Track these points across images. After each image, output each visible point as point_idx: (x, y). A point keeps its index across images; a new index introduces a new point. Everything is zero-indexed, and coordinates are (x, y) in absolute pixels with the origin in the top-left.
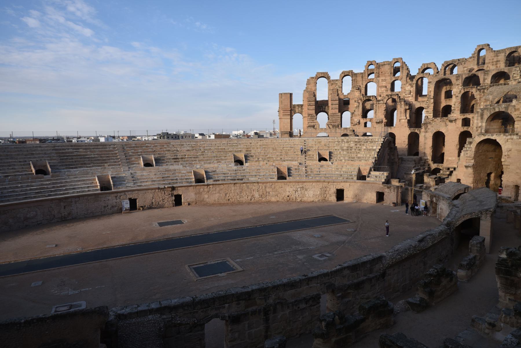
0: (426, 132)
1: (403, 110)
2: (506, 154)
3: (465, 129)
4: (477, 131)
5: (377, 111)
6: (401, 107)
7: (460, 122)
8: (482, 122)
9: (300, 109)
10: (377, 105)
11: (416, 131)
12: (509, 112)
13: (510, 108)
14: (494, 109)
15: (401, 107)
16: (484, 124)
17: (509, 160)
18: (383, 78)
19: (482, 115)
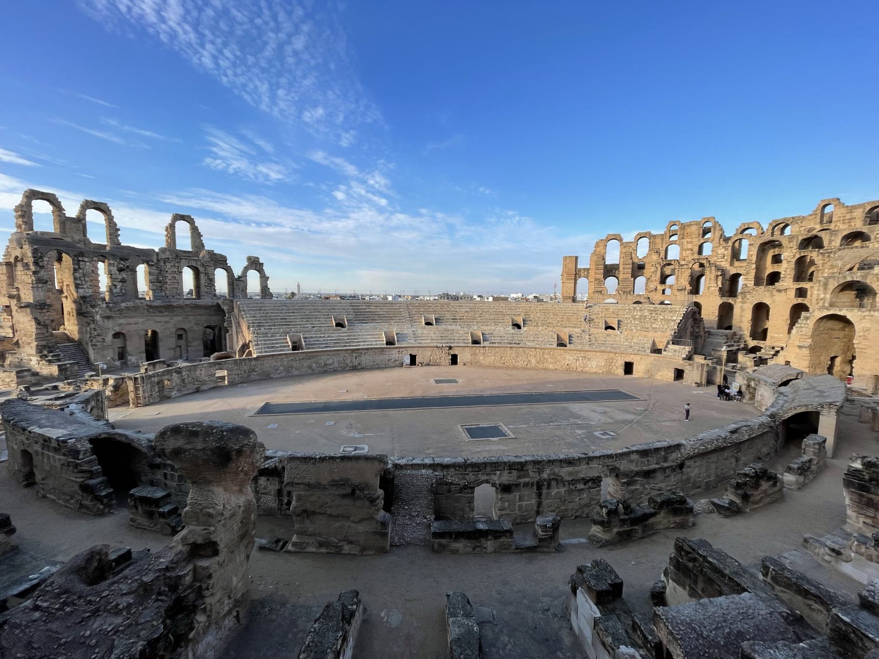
0: (744, 303)
1: (713, 276)
2: (862, 334)
7: (792, 293)
8: (825, 294)
13: (870, 277)
14: (845, 277)
16: (828, 296)
17: (865, 342)
19: (826, 285)
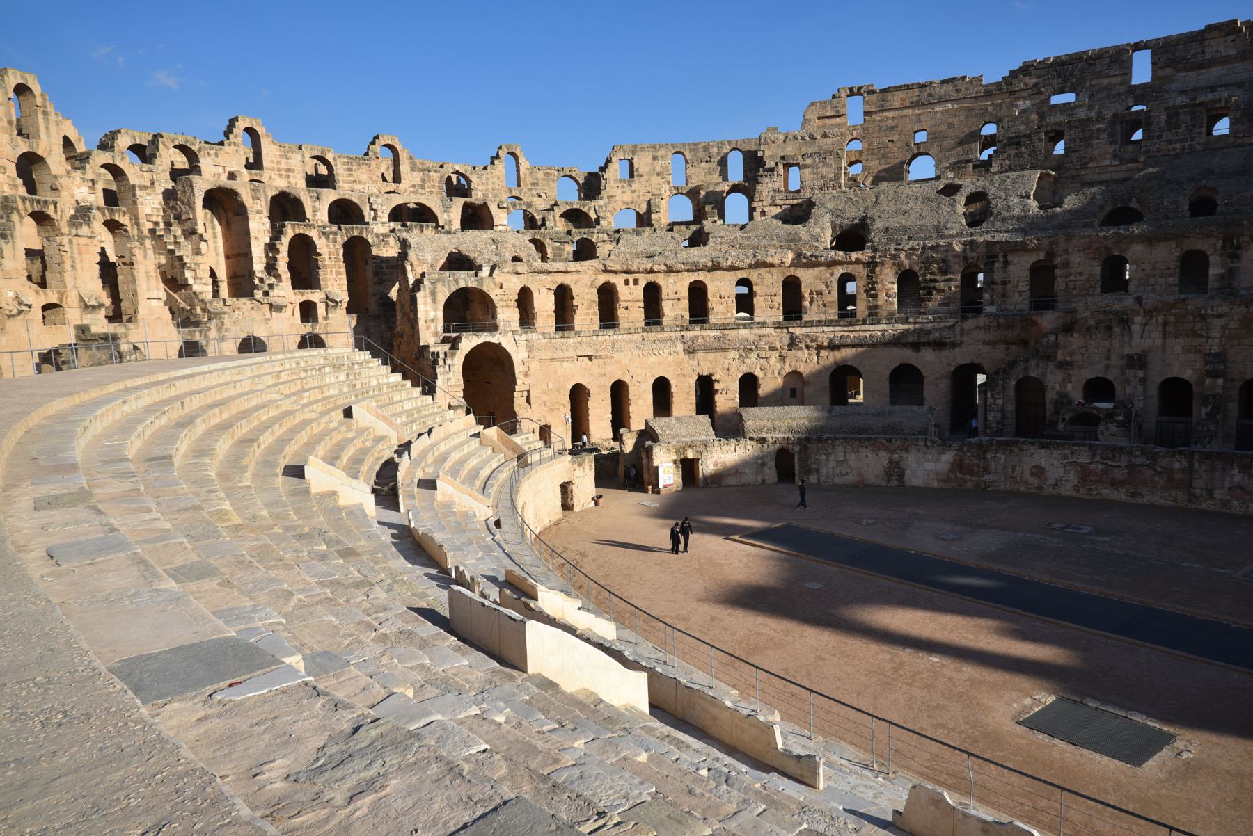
0: (223, 339)
3: (306, 329)
4: (428, 328)
5: (78, 266)
6: (145, 257)
8: (435, 310)
10: (75, 240)
11: (197, 337)
12: (485, 289)
13: (486, 282)
14: (457, 281)
15: (145, 257)
17: (528, 381)
19: (433, 294)
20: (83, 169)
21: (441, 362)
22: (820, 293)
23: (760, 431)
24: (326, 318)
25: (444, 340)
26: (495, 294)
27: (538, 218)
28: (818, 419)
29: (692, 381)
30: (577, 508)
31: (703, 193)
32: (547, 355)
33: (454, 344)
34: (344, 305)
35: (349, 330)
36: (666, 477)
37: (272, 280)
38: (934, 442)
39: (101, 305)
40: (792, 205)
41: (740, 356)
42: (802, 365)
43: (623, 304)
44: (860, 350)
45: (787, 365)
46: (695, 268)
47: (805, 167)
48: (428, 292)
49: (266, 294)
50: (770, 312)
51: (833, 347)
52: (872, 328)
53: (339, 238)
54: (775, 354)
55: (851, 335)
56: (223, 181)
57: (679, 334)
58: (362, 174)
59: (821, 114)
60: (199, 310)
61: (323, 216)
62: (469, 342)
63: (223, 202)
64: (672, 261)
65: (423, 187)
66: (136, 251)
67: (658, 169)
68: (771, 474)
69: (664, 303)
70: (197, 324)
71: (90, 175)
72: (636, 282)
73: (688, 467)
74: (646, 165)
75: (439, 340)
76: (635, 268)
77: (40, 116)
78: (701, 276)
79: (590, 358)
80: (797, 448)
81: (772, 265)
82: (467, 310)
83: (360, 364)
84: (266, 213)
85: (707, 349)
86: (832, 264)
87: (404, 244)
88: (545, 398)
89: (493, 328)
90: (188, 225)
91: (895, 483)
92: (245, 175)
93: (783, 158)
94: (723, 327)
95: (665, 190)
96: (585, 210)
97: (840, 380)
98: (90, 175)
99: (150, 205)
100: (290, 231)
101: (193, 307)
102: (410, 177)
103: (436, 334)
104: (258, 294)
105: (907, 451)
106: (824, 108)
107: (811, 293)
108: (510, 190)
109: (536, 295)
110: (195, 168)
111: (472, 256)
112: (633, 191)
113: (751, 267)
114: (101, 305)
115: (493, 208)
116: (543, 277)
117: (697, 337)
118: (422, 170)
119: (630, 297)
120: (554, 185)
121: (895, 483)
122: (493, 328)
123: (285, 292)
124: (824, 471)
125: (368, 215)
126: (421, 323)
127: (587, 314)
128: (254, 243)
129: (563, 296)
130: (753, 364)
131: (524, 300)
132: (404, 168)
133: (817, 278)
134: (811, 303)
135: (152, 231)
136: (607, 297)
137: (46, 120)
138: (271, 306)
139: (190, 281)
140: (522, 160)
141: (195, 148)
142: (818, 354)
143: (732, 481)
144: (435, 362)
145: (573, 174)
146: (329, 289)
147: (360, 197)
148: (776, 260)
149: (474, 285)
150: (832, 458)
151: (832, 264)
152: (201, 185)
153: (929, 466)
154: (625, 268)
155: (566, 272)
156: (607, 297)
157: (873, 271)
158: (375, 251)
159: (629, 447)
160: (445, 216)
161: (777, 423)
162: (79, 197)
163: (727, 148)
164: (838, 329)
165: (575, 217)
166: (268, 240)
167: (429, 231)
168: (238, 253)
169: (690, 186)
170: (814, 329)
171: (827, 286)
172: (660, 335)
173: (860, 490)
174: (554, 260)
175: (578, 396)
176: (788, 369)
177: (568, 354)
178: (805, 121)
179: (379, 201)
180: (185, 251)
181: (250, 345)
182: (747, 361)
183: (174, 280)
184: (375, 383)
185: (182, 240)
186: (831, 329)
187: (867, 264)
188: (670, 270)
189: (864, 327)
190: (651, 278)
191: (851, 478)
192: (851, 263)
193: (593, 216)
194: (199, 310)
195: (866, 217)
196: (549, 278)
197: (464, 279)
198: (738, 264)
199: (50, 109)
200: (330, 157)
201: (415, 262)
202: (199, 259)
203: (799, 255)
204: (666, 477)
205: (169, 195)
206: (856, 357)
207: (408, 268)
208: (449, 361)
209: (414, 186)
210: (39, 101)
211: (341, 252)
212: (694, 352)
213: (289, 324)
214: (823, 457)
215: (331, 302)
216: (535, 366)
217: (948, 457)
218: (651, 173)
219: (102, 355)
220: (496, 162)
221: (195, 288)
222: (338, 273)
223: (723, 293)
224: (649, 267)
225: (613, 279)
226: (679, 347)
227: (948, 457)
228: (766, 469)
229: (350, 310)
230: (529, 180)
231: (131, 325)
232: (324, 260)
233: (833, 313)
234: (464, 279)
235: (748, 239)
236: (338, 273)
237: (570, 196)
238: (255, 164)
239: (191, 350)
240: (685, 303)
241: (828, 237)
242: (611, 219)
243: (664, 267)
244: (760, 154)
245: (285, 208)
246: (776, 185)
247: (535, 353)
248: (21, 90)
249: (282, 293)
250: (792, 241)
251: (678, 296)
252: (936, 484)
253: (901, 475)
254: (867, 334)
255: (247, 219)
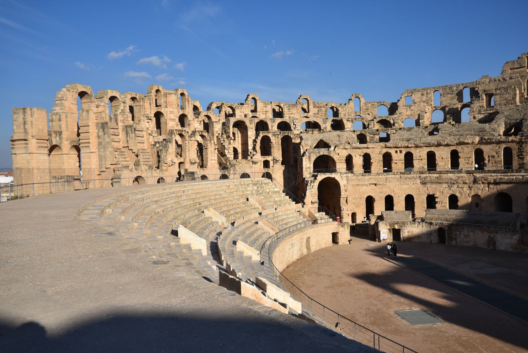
0: (235, 174)
1: (213, 149)
2: (344, 188)
3: (266, 170)
4: (307, 171)
5: (190, 150)
7: (260, 165)
8: (310, 164)
9: (58, 138)
10: (190, 142)
11: (226, 173)
12: (331, 155)
14: (319, 152)
17: (347, 193)
18: (171, 110)
19: (309, 158)
20: (198, 117)
21: (309, 184)
22: (493, 157)
23: (432, 219)
24: (273, 167)
25: (313, 176)
26: (335, 157)
27: (366, 124)
28: (460, 216)
29: (425, 197)
30: (340, 244)
31: (447, 109)
32: (356, 183)
33: (315, 177)
34: (280, 162)
35: (282, 171)
36: (384, 235)
37: (255, 153)
38: (510, 229)
39: (196, 162)
40: (490, 114)
41: (449, 186)
42: (480, 191)
43: (394, 161)
44: (510, 185)
45: (472, 192)
46: (429, 145)
47: (496, 94)
48: (307, 157)
49: (252, 158)
50: (467, 166)
51: (496, 183)
52: (516, 174)
53: (279, 136)
54: (467, 186)
55: (506, 178)
56: (242, 118)
57: (418, 176)
58: (294, 111)
59: (512, 67)
60: (228, 164)
61: (275, 128)
62: (321, 177)
63: (240, 125)
64: (418, 142)
65: (318, 114)
66: (209, 144)
67: (424, 100)
68: (435, 239)
69: (414, 161)
70: (227, 168)
71: (200, 119)
72: (401, 152)
73: (396, 233)
74: (418, 98)
75: (311, 175)
76: (399, 146)
77: (187, 102)
78: (432, 149)
79: (375, 185)
80: (447, 228)
81: (468, 144)
82: (324, 164)
83: (265, 184)
84: (254, 129)
85: (432, 183)
86: (499, 143)
87: (301, 138)
88: (354, 201)
89: (335, 171)
90: (228, 134)
91: (492, 248)
92: (251, 114)
93: (485, 91)
94: (440, 172)
95: (428, 109)
96: (388, 119)
97: (503, 200)
98: (200, 119)
99: (217, 128)
100: (261, 135)
101: (227, 162)
102: (313, 110)
103: (310, 173)
104: (249, 158)
105: (497, 233)
106: (514, 64)
107: (489, 157)
108: (356, 113)
109: (354, 158)
110: (233, 115)
111: (328, 142)
112: (411, 110)
113: (457, 144)
114: (196, 162)
115: (345, 121)
116: (357, 150)
117: (427, 177)
118: (318, 107)
119: (398, 158)
120: (376, 109)
121: (492, 248)
122: (335, 171)
123: (258, 157)
124: (458, 239)
125: (292, 126)
126: (304, 169)
127: (377, 166)
128: (249, 139)
129: (367, 158)
130: (455, 190)
131: (349, 160)
132: (311, 107)
133: (492, 149)
134: (489, 161)
135: (217, 137)
136: (387, 160)
137: (188, 103)
138: (253, 162)
139: (226, 154)
140: (362, 100)
141: (234, 107)
142: (488, 187)
143: (416, 240)
144: (307, 184)
145: (385, 104)
146: (275, 155)
147: (290, 121)
148: (470, 141)
149: (327, 154)
150: (462, 233)
151: (499, 143)
152: (232, 120)
153: (508, 241)
154: (395, 146)
155: (368, 148)
156: (387, 160)
157: (521, 146)
158: (293, 141)
159: (373, 222)
160: (324, 125)
161: (441, 216)
162: (196, 127)
163: (461, 87)
164: (499, 174)
165: (385, 123)
166: (254, 138)
167: (316, 132)
168: (245, 144)
169: (442, 106)
170: (487, 174)
171: (497, 154)
172: (409, 176)
173: (475, 249)
174: (370, 142)
175: (370, 201)
176: (473, 193)
177: (365, 183)
178: (503, 72)
179: (297, 121)
180: (226, 144)
181: (245, 176)
182: (452, 188)
183: (222, 154)
184: (268, 190)
185: (226, 139)
186: (495, 174)
187: (518, 143)
188: (417, 147)
189: (512, 174)
190: (408, 150)
191: (471, 244)
192: (509, 142)
193: (392, 122)
194: (228, 164)
195: (523, 119)
196: (360, 150)
197: (323, 151)
198: (450, 143)
199: (190, 100)
200: (282, 105)
201: (304, 145)
202: (230, 146)
203: (482, 139)
204: (384, 235)
205: (224, 124)
206: (508, 189)
207: (301, 147)
208: (312, 184)
209: (314, 114)
210: (187, 97)
211: (280, 142)
212: (425, 183)
213: (259, 168)
214: (458, 233)
215: (275, 161)
216: (350, 187)
217: (516, 237)
218: (420, 102)
219: (190, 178)
220: (350, 101)
221: (228, 156)
222: (279, 150)
223: (443, 157)
224: (406, 145)
225: (390, 150)
226: (418, 181)
227: (516, 237)
228: (432, 237)
229: (282, 164)
230: (364, 108)
231: (205, 169)
232: (273, 145)
233: (501, 166)
234: (323, 151)
235: (459, 131)
236: (279, 150)
237: (384, 113)
238: (255, 111)
239: (224, 177)
240: (425, 161)
241: (502, 130)
242: (401, 123)
243: (413, 145)
244: (476, 89)
245: (262, 126)
246: (481, 104)
247: (350, 182)
248: (182, 94)
249: (257, 157)
250: (481, 131)
251: (421, 158)
252: (511, 250)
253: (495, 244)
254: (514, 177)
255: (247, 131)
